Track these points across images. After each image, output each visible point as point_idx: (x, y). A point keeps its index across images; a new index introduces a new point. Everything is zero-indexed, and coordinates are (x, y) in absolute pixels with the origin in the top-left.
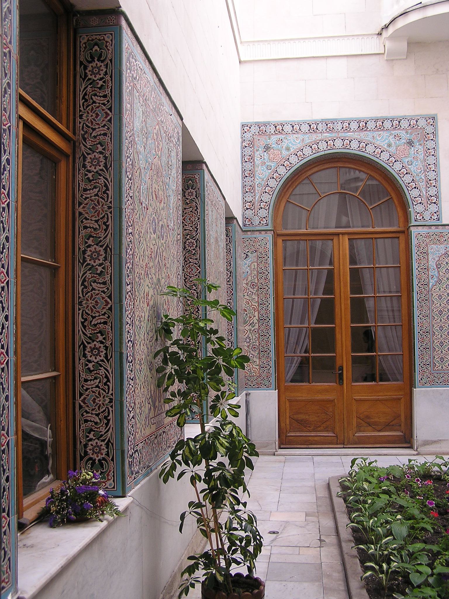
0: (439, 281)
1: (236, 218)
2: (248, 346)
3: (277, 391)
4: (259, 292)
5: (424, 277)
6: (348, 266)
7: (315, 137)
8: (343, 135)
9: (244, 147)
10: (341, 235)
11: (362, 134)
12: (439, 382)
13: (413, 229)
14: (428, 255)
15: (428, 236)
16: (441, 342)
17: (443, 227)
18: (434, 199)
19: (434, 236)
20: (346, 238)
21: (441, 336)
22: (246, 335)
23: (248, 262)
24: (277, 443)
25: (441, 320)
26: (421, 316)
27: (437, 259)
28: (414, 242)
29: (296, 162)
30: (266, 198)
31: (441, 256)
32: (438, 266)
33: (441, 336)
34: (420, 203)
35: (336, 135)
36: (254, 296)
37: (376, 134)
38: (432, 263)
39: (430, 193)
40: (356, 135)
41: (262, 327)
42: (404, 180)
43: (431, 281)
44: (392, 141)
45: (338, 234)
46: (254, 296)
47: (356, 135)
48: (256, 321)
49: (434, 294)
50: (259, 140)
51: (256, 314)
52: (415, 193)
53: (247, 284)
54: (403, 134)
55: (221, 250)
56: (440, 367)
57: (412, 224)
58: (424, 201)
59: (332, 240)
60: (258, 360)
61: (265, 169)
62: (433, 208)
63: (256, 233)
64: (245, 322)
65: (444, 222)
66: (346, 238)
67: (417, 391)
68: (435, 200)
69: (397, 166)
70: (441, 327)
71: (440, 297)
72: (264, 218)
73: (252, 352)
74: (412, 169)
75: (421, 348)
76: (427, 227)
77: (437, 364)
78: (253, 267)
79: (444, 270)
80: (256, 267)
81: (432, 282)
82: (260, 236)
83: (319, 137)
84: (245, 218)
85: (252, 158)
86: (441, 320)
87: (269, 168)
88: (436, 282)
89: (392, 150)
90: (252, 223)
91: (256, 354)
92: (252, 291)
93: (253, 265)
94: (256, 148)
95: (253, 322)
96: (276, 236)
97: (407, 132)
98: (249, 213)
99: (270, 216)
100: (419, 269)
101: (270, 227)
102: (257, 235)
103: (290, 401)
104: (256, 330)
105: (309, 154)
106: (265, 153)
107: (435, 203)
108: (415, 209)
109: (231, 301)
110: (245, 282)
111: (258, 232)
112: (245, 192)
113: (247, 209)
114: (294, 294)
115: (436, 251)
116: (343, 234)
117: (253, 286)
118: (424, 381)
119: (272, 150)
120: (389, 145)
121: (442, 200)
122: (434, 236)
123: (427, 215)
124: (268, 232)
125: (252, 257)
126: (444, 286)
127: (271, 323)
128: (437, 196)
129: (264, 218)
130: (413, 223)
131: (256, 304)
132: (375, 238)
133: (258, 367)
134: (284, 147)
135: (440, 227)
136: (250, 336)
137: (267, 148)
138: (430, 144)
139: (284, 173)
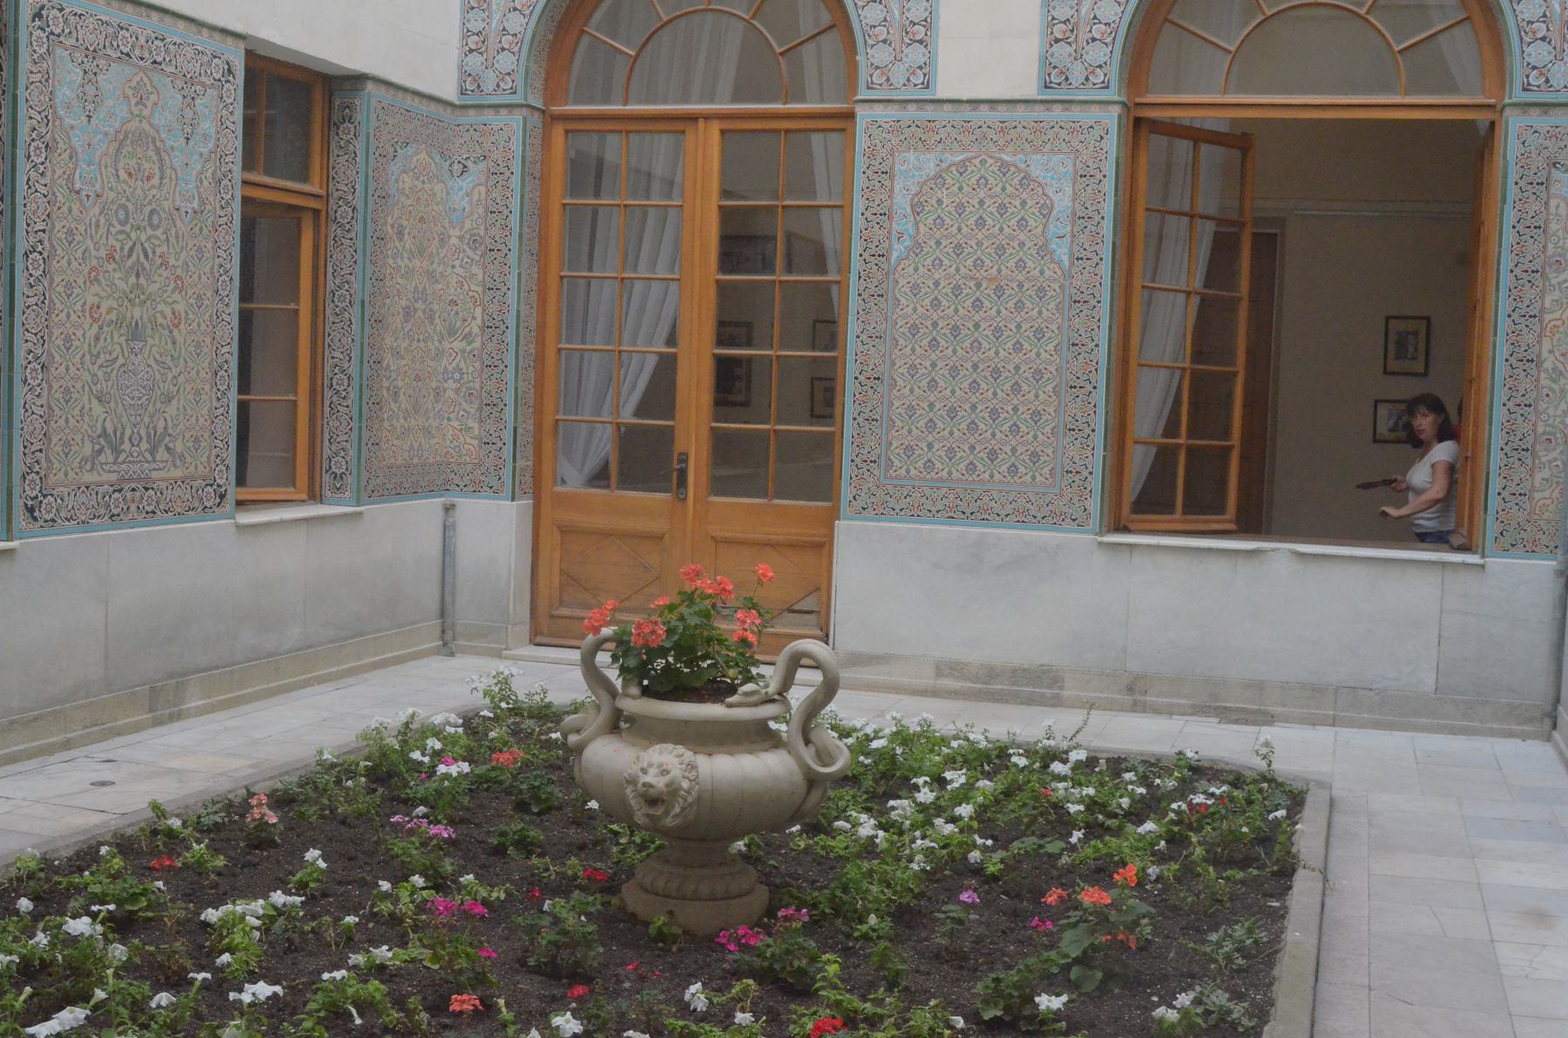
0: (917, 248)
2: (457, 391)
3: (528, 502)
5: (879, 234)
6: (715, 201)
10: (701, 123)
12: (898, 508)
14: (892, 178)
15: (897, 127)
16: (911, 407)
17: (937, 106)
18: (920, 32)
19: (913, 128)
20: (715, 128)
21: (912, 391)
23: (466, 183)
24: (525, 630)
25: (913, 350)
26: (863, 337)
27: (914, 190)
28: (861, 142)
31: (925, 183)
32: (917, 208)
33: (912, 391)
34: (884, 41)
36: (475, 269)
38: (902, 202)
39: (912, 16)
41: (491, 346)
43: (896, 246)
45: (692, 118)
46: (475, 269)
48: (476, 330)
49: (902, 282)
51: (479, 311)
53: (461, 238)
56: (903, 471)
57: (859, 97)
58: (895, 36)
59: (683, 132)
60: (476, 426)
62: (916, 55)
63: (486, 111)
64: (452, 332)
65: (941, 94)
66: (715, 128)
67: (841, 525)
68: (922, 33)
70: (913, 366)
71: (915, 289)
73: (465, 406)
75: (860, 420)
76: (897, 106)
77: (897, 463)
78: (476, 197)
79: (930, 221)
81: (898, 250)
82: (495, 120)
84: (464, 74)
86: (913, 350)
88: (909, 249)
95: (470, 333)
96: (551, 119)
98: (475, 61)
99: (522, 71)
100: (868, 214)
102: (489, 116)
103: (565, 531)
107: (921, 42)
108: (872, 56)
109: (352, 278)
110: (457, 232)
111: (492, 111)
113: (471, 51)
114: (590, 269)
115: (914, 168)
116: (708, 117)
117: (475, 242)
118: (859, 503)
121: (941, 33)
122: (913, 128)
123: (898, 75)
124: (515, 111)
125: (477, 171)
126: (929, 261)
127: (510, 336)
128: (928, 23)
130: (863, 94)
131: (480, 289)
132: (787, 131)
133: (476, 442)
135: (930, 107)
136: (462, 365)
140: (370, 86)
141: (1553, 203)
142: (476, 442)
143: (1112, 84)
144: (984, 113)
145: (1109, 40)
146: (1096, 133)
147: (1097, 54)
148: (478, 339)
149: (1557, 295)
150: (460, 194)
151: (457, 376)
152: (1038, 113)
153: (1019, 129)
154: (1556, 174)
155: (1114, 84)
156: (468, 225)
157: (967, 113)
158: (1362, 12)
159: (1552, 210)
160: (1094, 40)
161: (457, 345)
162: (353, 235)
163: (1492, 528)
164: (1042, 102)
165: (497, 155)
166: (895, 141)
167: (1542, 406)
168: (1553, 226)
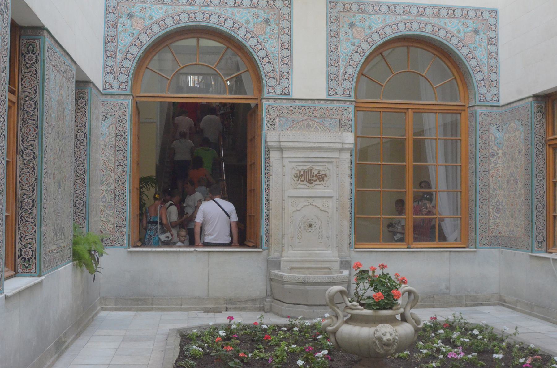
1: (92, 83)
2: (104, 206)
4: (117, 154)
7: (177, 9)
8: (204, 8)
9: (107, 13)
11: (222, 9)
13: (264, 102)
22: (102, 196)
23: (106, 123)
29: (158, 31)
30: (127, 63)
34: (273, 78)
35: (198, 8)
36: (111, 158)
37: (236, 10)
40: (217, 10)
42: (259, 56)
44: (251, 19)
47: (217, 10)
48: (112, 182)
50: (123, 7)
51: (113, 174)
52: (268, 68)
54: (261, 12)
55: (67, 112)
60: (113, 220)
61: (128, 36)
62: (285, 83)
64: (102, 182)
69: (253, 42)
72: (124, 83)
74: (267, 47)
80: (114, 129)
83: (182, 8)
85: (115, 24)
87: (131, 35)
89: (250, 26)
90: (112, 87)
91: (111, 214)
92: (110, 152)
93: (111, 127)
94: (120, 15)
95: (109, 183)
97: (264, 11)
98: (110, 78)
101: (128, 92)
102: (116, 99)
104: (112, 191)
105: (171, 25)
106: (129, 21)
108: (268, 83)
110: (102, 143)
112: (106, 57)
119: (135, 18)
120: (248, 22)
123: (278, 89)
124: (128, 97)
129: (124, 83)
130: (265, 96)
134: (147, 16)
136: (106, 195)
137: (131, 16)
138: (285, 24)
139: (146, 40)
140: (91, 85)
141: (490, 135)
142: (112, 226)
143: (352, 95)
144: (310, 104)
145: (351, 80)
146: (347, 111)
147: (347, 84)
148: (113, 185)
149: (493, 165)
150: (104, 128)
151: (104, 200)
152: (329, 104)
153: (322, 109)
154: (490, 126)
155: (353, 95)
156: (108, 140)
157: (303, 104)
158: (424, 75)
159: (490, 138)
160: (346, 80)
161: (104, 188)
162: (85, 144)
163: (478, 240)
164: (330, 100)
165: (120, 113)
166: (278, 113)
167: (490, 199)
168: (491, 143)
